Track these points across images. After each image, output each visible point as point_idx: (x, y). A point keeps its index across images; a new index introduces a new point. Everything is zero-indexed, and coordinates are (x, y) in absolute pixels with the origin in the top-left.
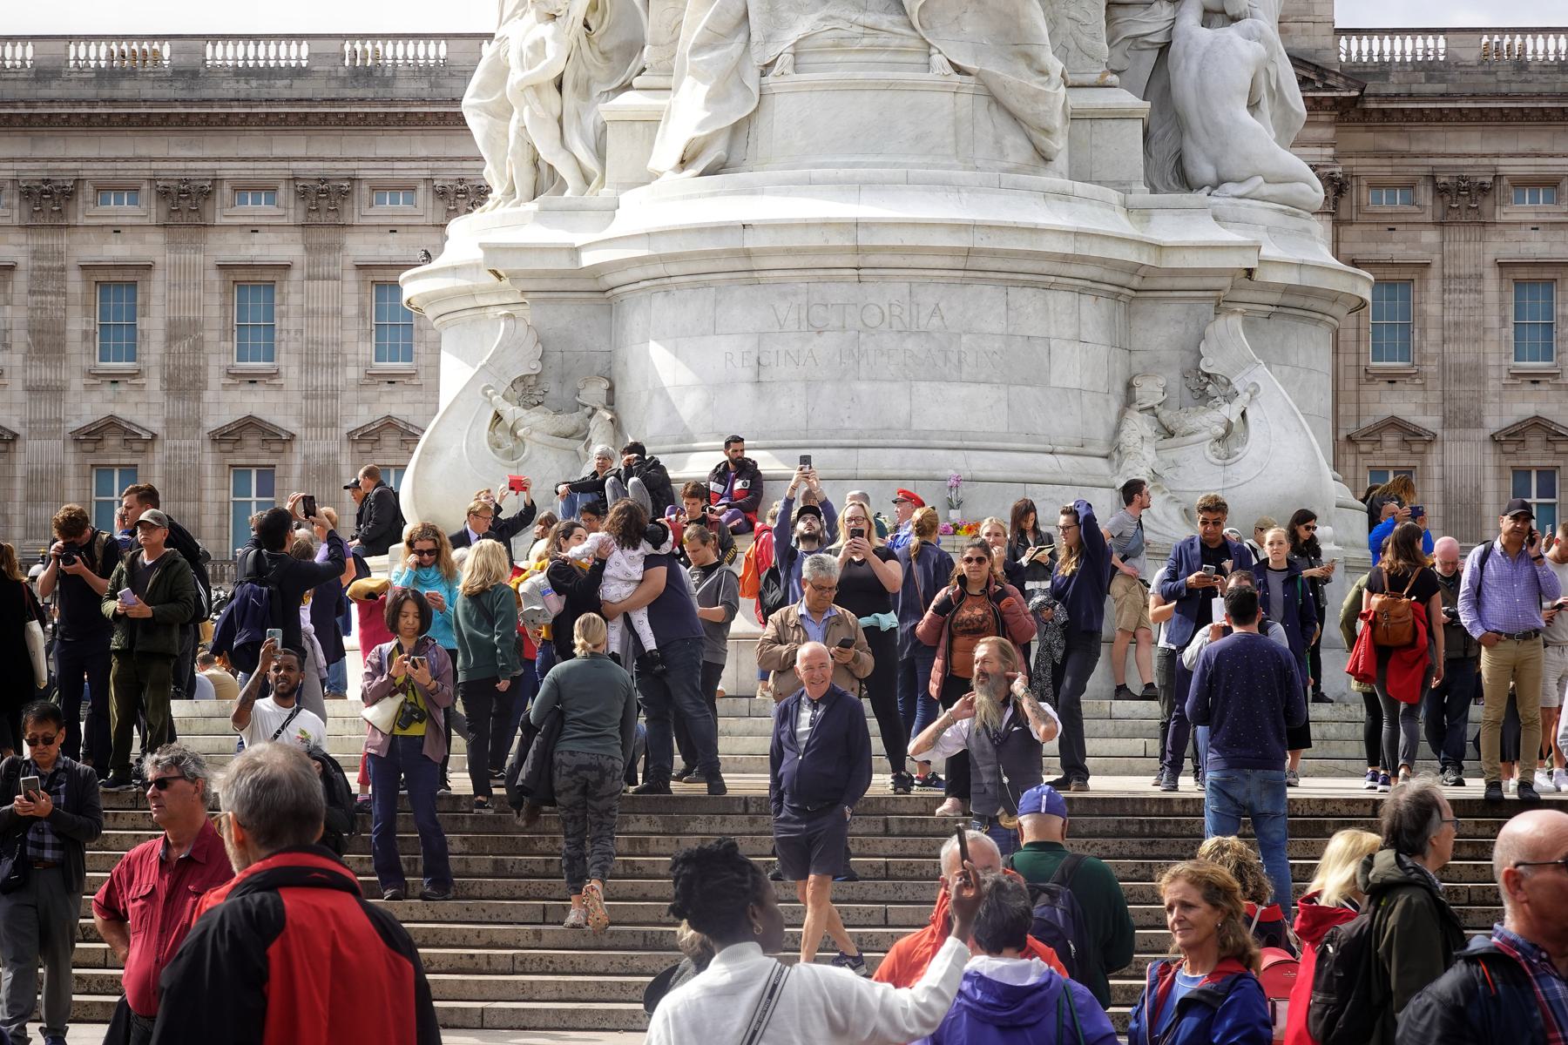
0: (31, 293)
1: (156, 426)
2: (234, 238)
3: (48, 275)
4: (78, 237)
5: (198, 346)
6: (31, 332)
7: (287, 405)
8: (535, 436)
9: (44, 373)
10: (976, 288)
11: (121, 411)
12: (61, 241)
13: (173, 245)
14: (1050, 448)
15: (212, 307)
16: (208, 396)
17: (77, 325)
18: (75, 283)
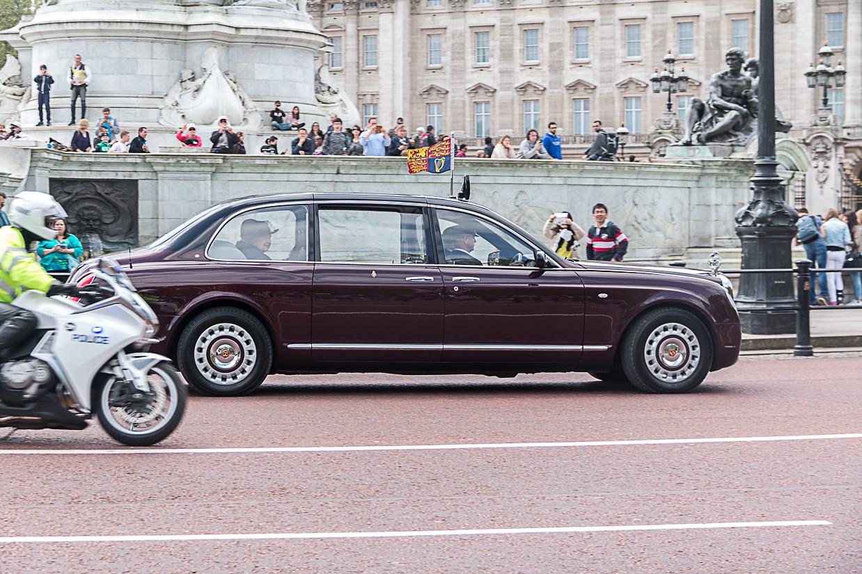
0: (501, 35)
1: (546, 85)
2: (574, 10)
3: (507, 27)
4: (517, 12)
5: (561, 53)
6: (501, 50)
7: (594, 75)
8: (8, 96)
9: (506, 66)
10: (107, 42)
11: (533, 80)
12: (510, 15)
13: (551, 15)
14: (136, 96)
15: (567, 39)
16: (564, 72)
17: (517, 46)
18: (517, 31)
